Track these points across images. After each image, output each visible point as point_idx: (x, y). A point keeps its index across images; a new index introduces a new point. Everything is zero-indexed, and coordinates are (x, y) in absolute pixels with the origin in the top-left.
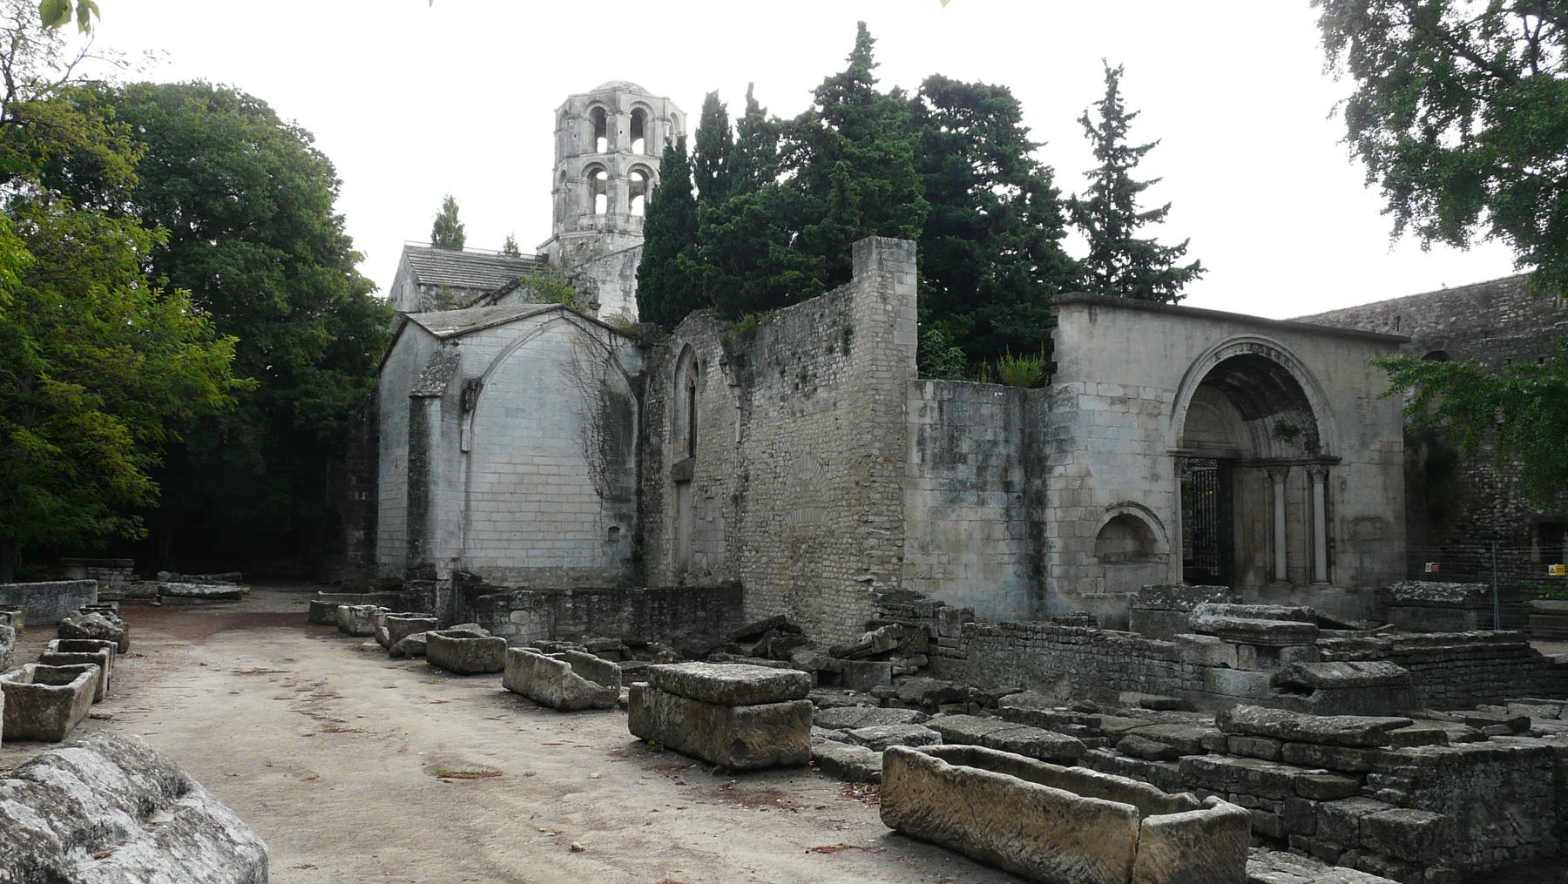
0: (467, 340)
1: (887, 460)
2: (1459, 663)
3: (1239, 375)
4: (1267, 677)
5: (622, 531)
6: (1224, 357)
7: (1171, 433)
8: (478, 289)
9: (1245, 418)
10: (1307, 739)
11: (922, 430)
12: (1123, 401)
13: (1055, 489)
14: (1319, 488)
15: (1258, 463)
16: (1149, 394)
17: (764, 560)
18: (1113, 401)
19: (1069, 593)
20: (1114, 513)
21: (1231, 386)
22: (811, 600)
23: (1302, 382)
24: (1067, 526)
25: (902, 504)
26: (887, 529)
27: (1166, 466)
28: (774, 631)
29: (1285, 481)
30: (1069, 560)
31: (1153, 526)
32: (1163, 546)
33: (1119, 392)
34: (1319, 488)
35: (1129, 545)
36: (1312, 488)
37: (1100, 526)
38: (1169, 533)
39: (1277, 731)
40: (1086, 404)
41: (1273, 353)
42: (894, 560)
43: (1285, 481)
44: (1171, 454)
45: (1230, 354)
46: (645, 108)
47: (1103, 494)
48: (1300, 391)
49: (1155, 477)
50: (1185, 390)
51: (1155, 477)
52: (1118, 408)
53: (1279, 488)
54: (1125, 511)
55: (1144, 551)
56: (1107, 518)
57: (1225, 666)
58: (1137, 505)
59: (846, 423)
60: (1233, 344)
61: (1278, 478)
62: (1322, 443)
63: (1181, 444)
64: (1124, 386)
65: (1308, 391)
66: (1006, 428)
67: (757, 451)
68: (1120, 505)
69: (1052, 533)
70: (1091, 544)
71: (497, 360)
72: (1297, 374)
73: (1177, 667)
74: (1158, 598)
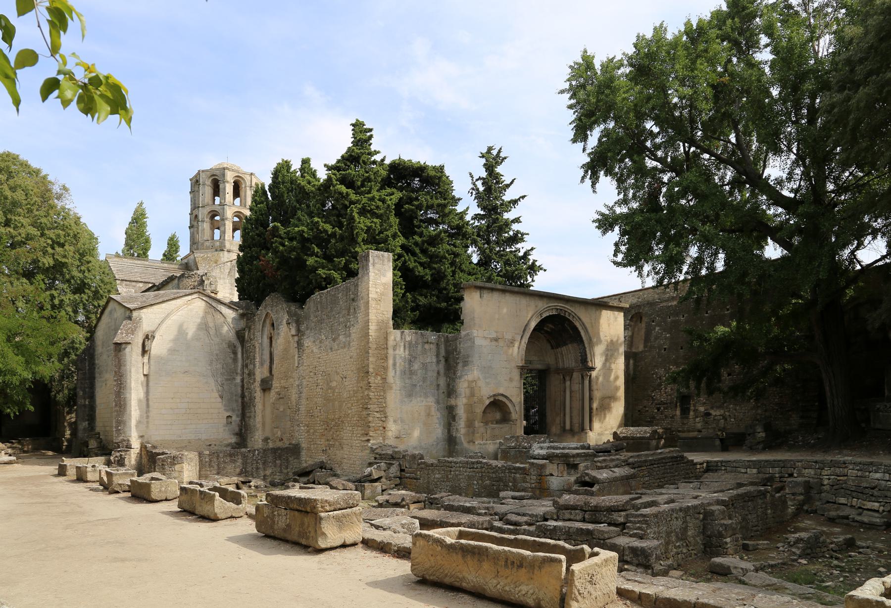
0: (144, 310)
2: (655, 466)
3: (551, 326)
4: (573, 479)
5: (234, 418)
6: (544, 316)
8: (149, 283)
9: (552, 348)
10: (596, 509)
12: (496, 340)
13: (462, 386)
14: (587, 382)
15: (558, 371)
16: (508, 336)
17: (312, 431)
19: (469, 442)
20: (492, 399)
21: (547, 332)
22: (338, 452)
23: (580, 329)
24: (470, 408)
25: (385, 398)
26: (377, 412)
27: (516, 375)
28: (319, 469)
29: (570, 380)
30: (470, 424)
31: (510, 405)
33: (494, 335)
35: (498, 416)
37: (485, 406)
38: (517, 409)
39: (582, 507)
40: (478, 342)
41: (567, 314)
42: (381, 428)
43: (570, 380)
47: (486, 392)
48: (579, 332)
49: (511, 380)
50: (526, 333)
52: (494, 343)
53: (568, 383)
54: (497, 398)
55: (505, 418)
56: (487, 402)
57: (552, 475)
58: (502, 395)
59: (355, 354)
61: (567, 378)
62: (589, 359)
63: (524, 362)
64: (497, 332)
65: (583, 334)
66: (437, 356)
67: (307, 371)
68: (494, 395)
69: (461, 412)
71: (162, 322)
72: (577, 324)
73: (528, 477)
74: (513, 442)
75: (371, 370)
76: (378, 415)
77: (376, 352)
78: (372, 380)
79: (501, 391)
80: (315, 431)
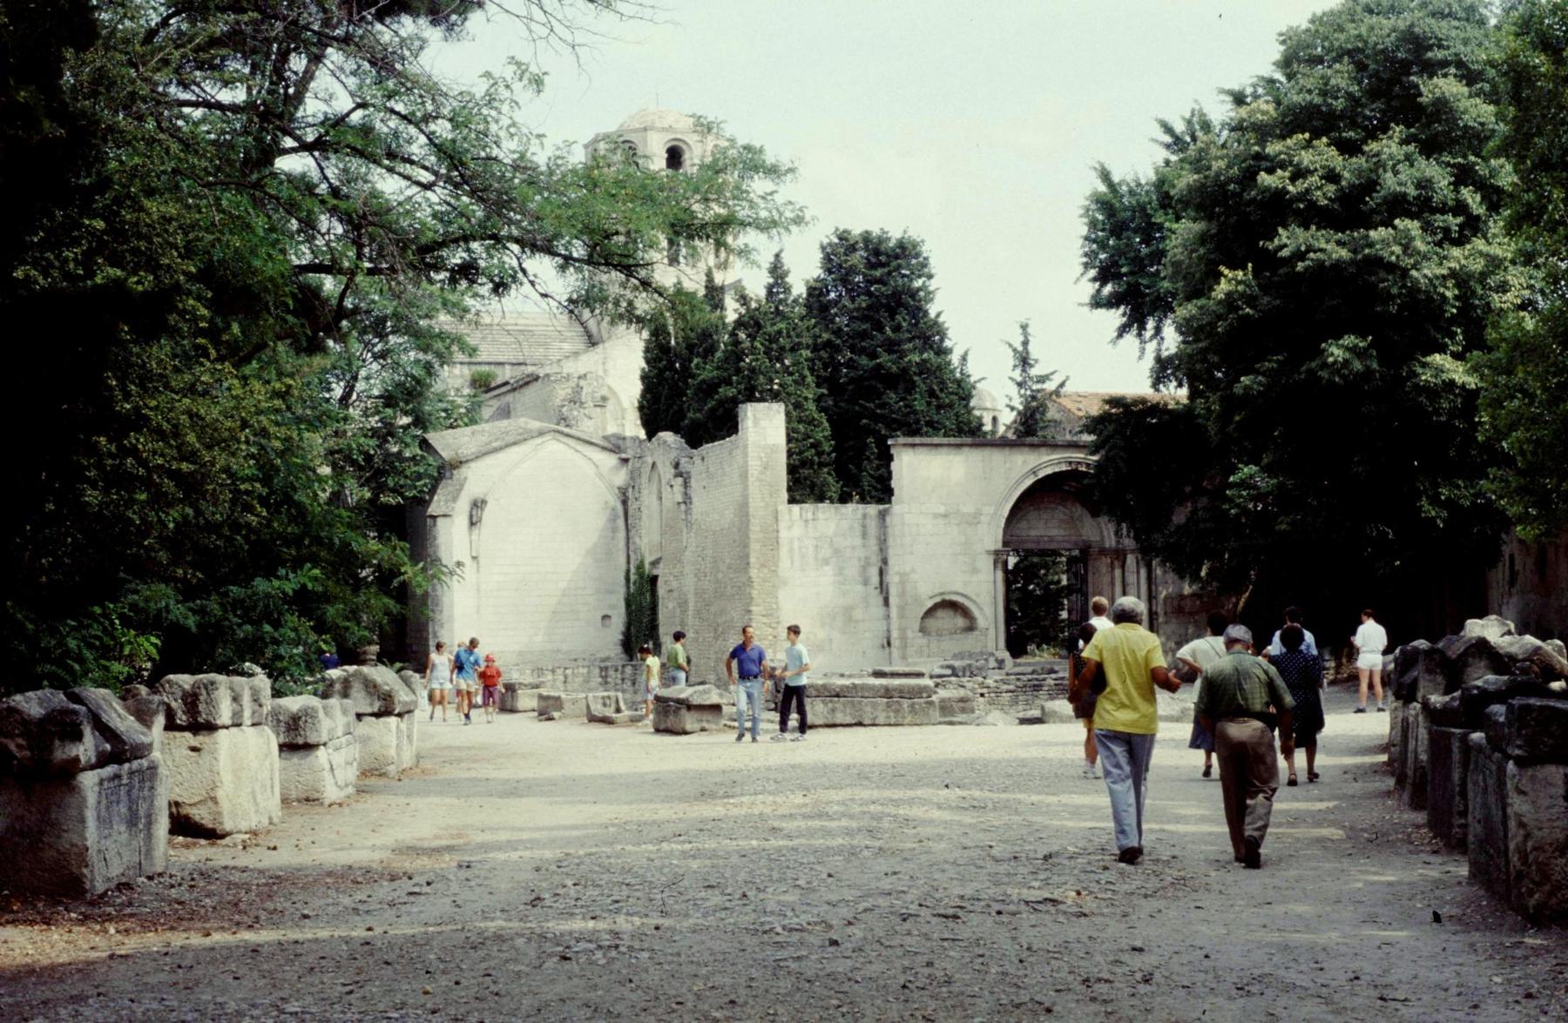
1: (763, 565)
6: (1041, 474)
7: (992, 535)
11: (791, 542)
12: (945, 516)
16: (968, 509)
18: (936, 516)
20: (938, 599)
27: (986, 563)
32: (981, 622)
33: (942, 510)
34: (1143, 572)
35: (960, 622)
36: (1138, 572)
38: (989, 611)
44: (988, 552)
45: (1049, 471)
46: (680, 144)
47: (927, 590)
51: (975, 571)
52: (941, 521)
53: (1118, 572)
56: (930, 604)
58: (958, 593)
60: (1050, 463)
66: (864, 535)
68: (942, 594)
70: (917, 626)
75: (752, 560)
76: (765, 620)
77: (761, 535)
78: (754, 572)
79: (959, 587)
80: (704, 639)
